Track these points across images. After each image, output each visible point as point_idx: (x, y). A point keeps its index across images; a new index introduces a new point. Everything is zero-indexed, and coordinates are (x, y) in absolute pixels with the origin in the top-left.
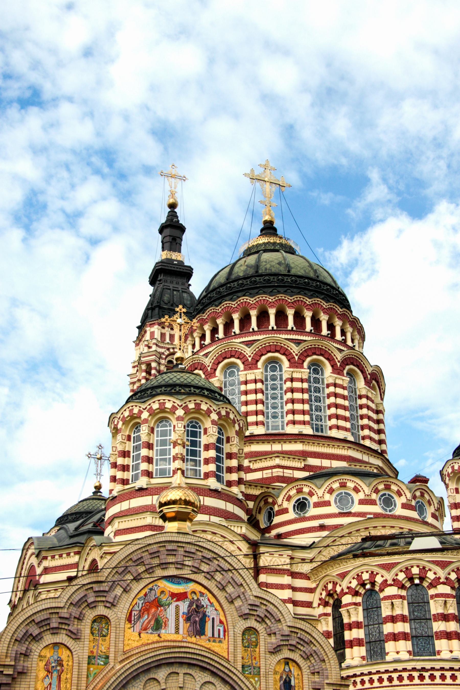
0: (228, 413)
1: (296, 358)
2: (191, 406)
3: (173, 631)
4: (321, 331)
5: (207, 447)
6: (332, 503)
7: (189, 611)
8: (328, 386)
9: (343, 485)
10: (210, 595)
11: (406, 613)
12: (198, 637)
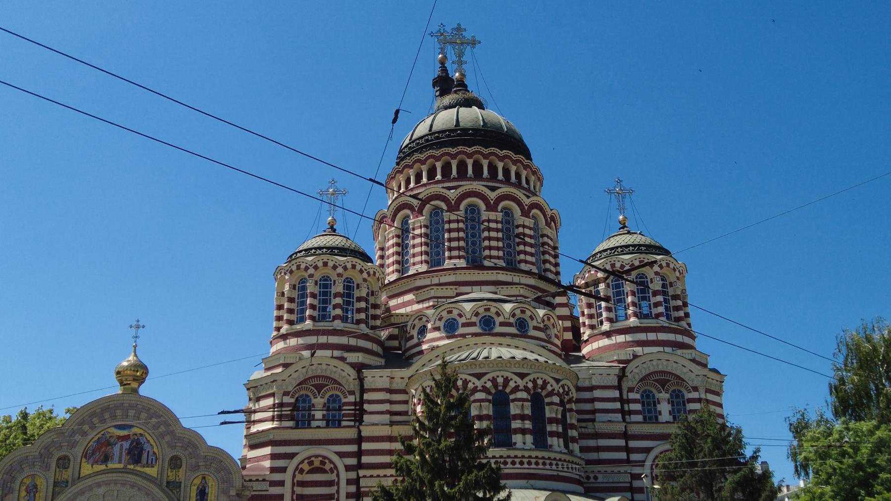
0: (354, 267)
1: (453, 202)
3: (117, 461)
5: (337, 295)
6: (442, 328)
7: (130, 448)
10: (147, 436)
11: (491, 413)
12: (135, 465)
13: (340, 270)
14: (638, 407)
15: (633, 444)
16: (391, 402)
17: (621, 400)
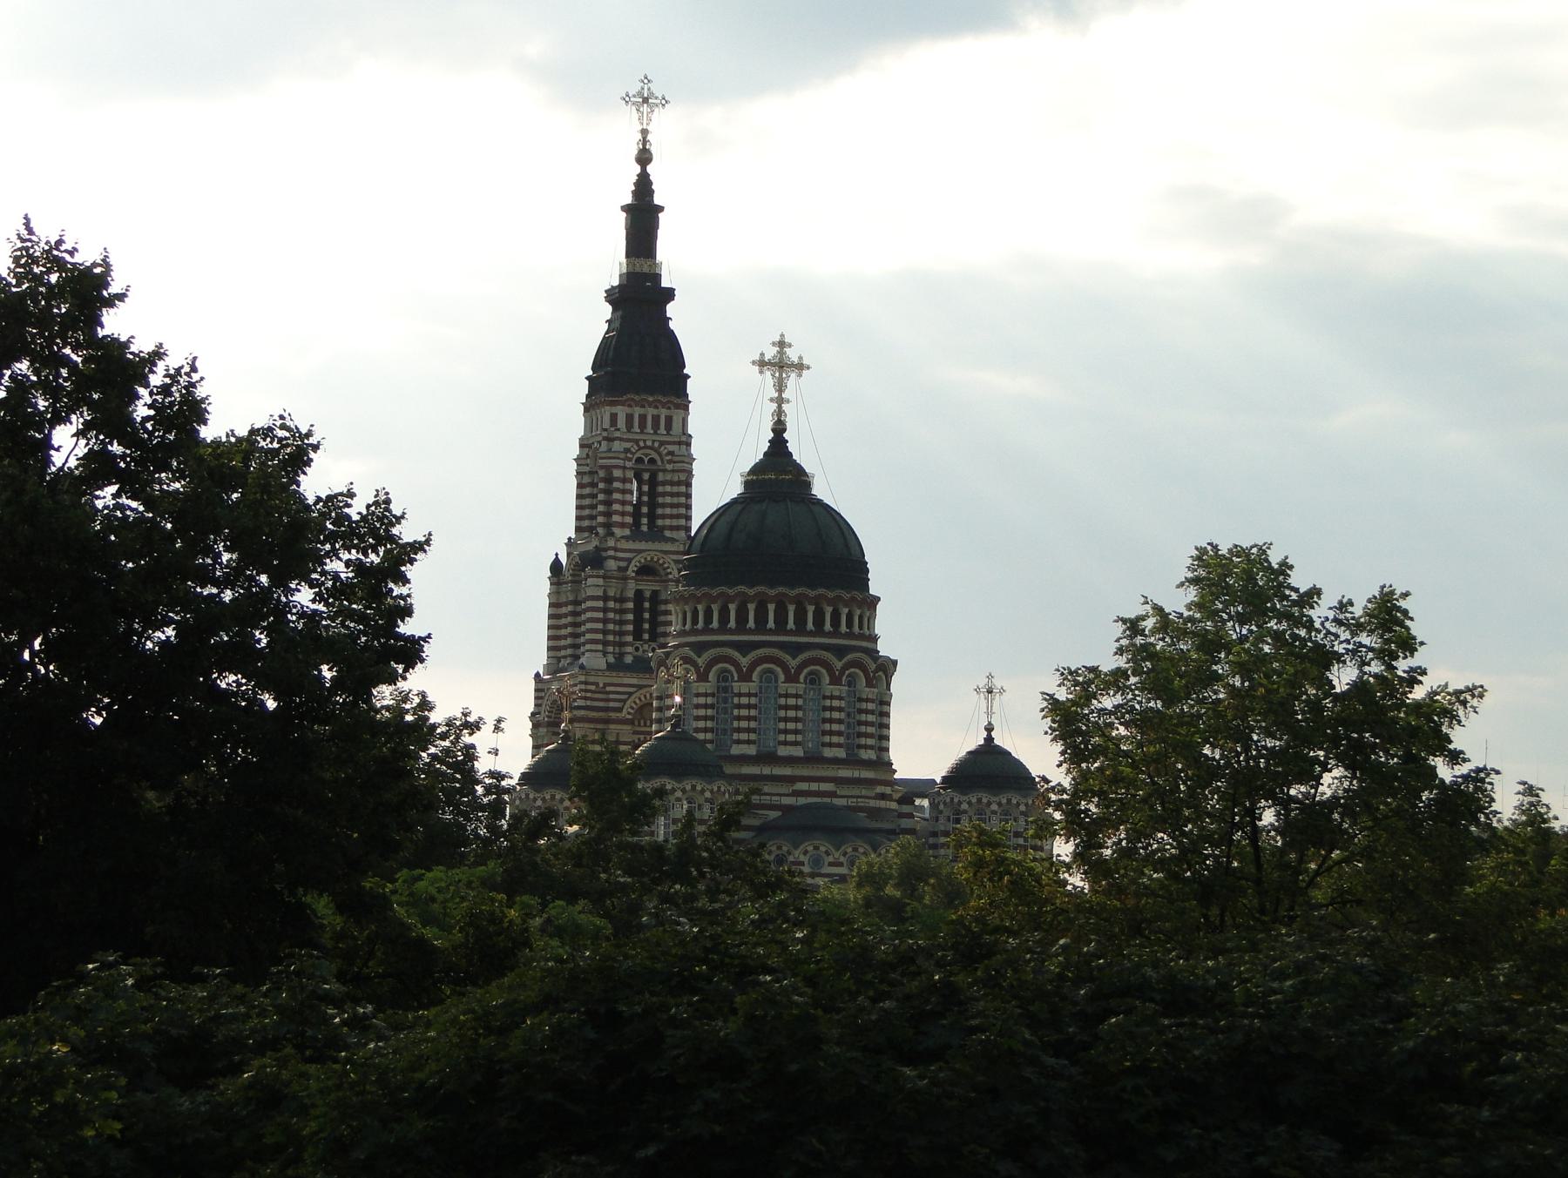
0: (719, 788)
1: (793, 671)
2: (688, 787)
4: (824, 625)
8: (825, 697)
9: (816, 848)
13: (708, 795)
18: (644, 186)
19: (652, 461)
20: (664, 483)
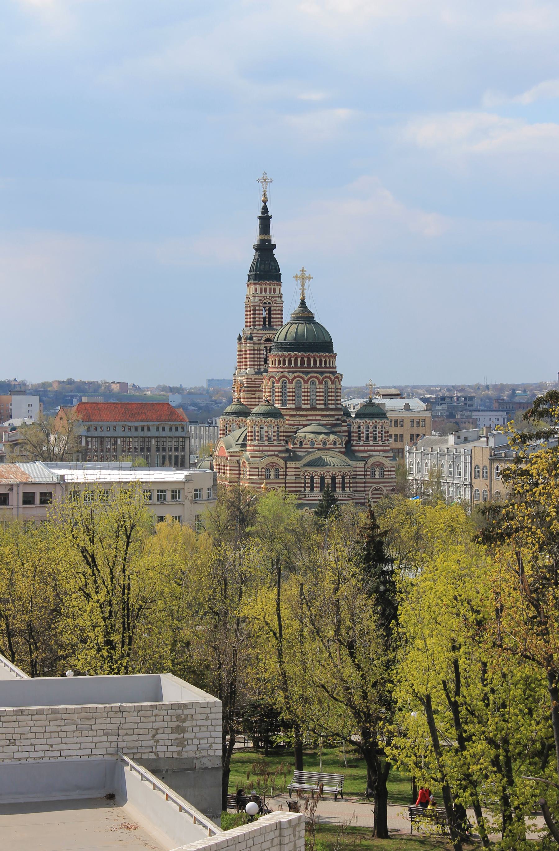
4: (316, 364)
14: (369, 473)
15: (367, 485)
16: (295, 471)
17: (365, 471)
18: (265, 210)
19: (269, 303)
20: (273, 311)
